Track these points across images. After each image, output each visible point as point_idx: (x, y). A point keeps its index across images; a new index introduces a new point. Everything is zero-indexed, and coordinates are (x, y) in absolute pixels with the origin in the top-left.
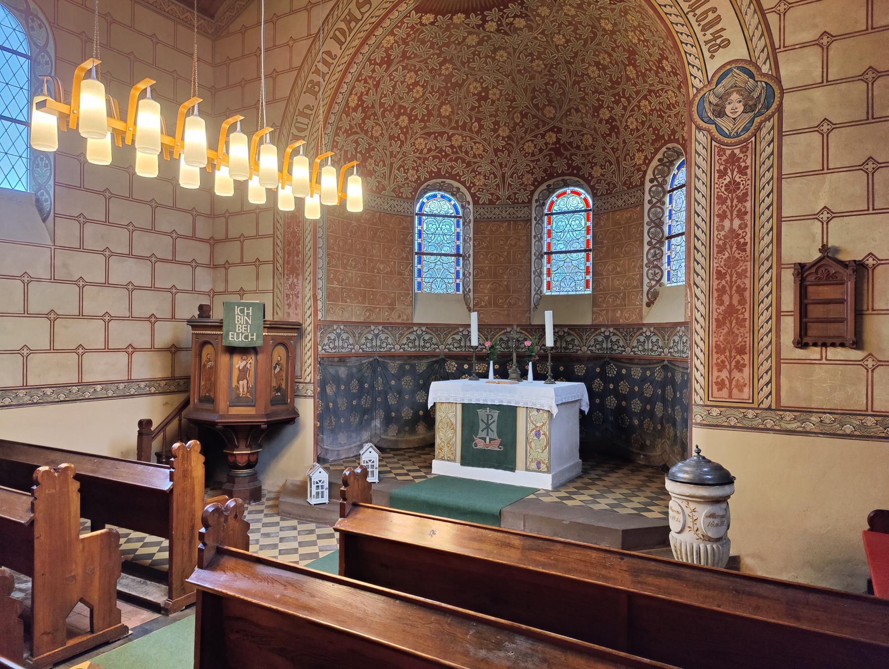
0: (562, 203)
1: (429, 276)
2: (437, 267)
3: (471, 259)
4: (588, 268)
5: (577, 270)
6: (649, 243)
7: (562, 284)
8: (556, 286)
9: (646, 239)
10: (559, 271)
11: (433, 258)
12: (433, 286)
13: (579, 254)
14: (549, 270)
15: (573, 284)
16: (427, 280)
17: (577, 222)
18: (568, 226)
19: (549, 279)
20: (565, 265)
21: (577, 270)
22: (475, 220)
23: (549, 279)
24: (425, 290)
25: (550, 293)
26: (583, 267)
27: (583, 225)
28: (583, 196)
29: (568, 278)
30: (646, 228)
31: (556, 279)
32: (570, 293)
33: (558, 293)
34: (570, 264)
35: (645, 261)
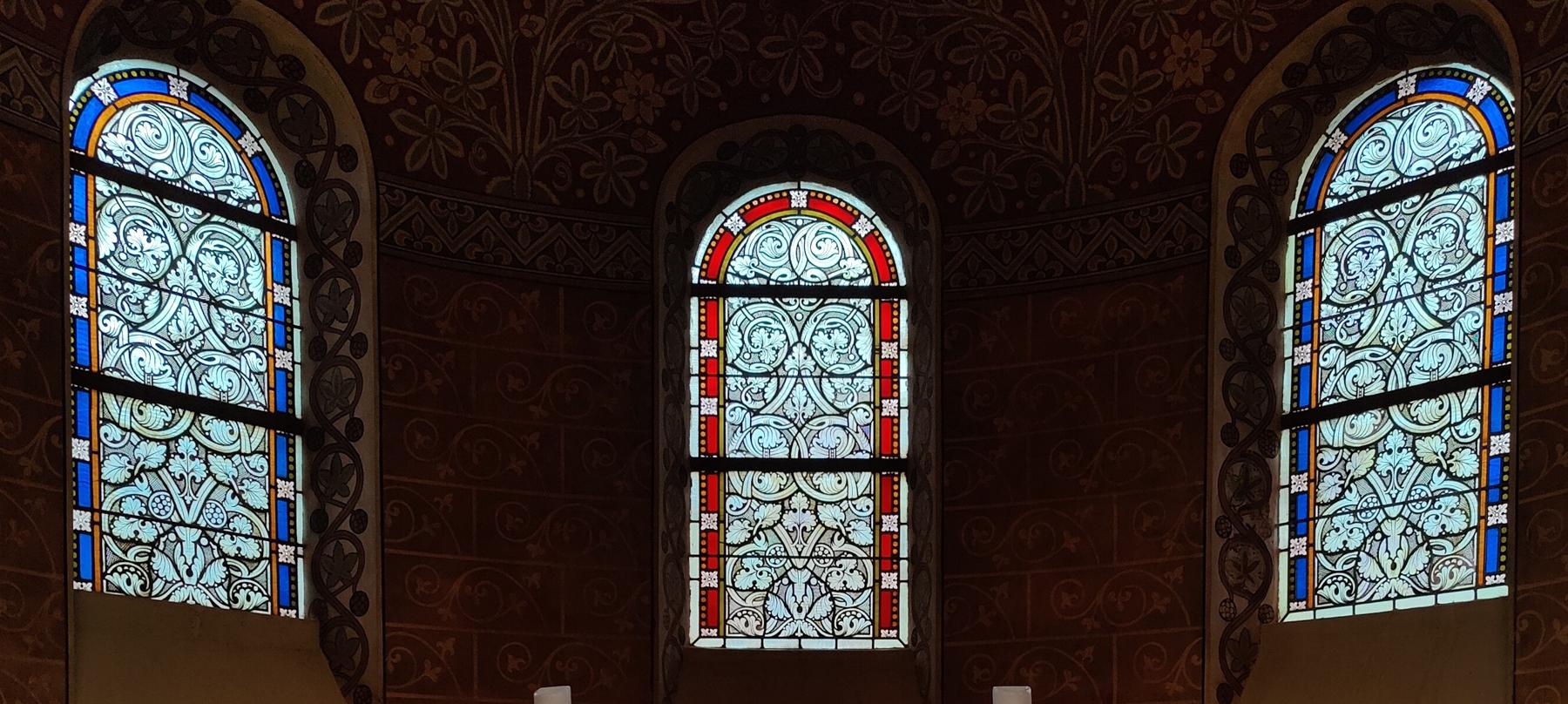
0: (769, 246)
1: (132, 507)
2: (176, 466)
3: (366, 448)
4: (889, 539)
5: (839, 545)
6: (1229, 434)
7: (775, 606)
8: (744, 613)
9: (1220, 415)
10: (760, 545)
11: (155, 415)
12: (161, 564)
13: (849, 476)
14: (709, 537)
15: (824, 606)
16: (124, 529)
17: (840, 338)
18: (799, 351)
19: (711, 580)
20: (790, 520)
21: (839, 545)
22: (387, 254)
23: (711, 580)
24: (118, 580)
25: (716, 643)
26: (864, 535)
27: (867, 355)
28: (862, 228)
29: (799, 578)
30: (1219, 368)
31: (743, 581)
32: (807, 645)
33: (755, 644)
34: (809, 520)
35: (1216, 511)
